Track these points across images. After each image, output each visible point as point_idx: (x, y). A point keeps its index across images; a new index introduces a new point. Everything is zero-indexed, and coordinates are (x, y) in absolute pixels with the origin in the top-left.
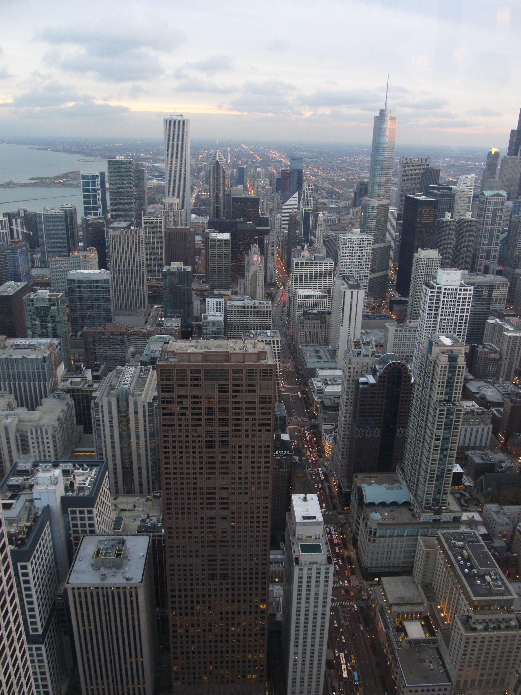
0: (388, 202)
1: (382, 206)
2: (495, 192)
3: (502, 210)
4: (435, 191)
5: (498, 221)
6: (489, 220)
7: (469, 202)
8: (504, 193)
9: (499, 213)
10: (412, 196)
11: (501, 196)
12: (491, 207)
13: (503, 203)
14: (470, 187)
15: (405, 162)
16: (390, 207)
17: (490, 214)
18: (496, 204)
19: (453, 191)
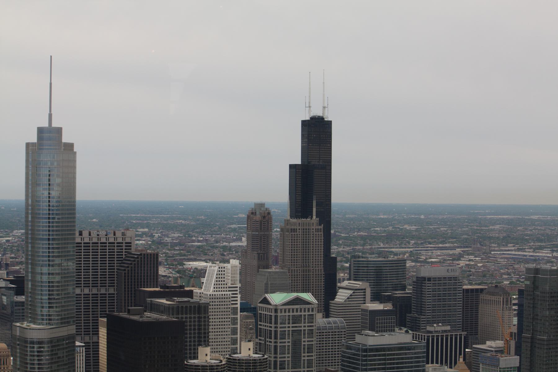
0: (72, 329)
1: (59, 339)
2: (294, 295)
3: (311, 332)
4: (164, 301)
5: (305, 357)
6: (288, 357)
7: (234, 322)
8: (307, 296)
9: (305, 341)
10: (124, 315)
11: (308, 303)
12: (289, 327)
13: (311, 317)
14: (232, 288)
15: (78, 240)
16: (78, 343)
17: (288, 342)
18: (296, 320)
19: (196, 299)
